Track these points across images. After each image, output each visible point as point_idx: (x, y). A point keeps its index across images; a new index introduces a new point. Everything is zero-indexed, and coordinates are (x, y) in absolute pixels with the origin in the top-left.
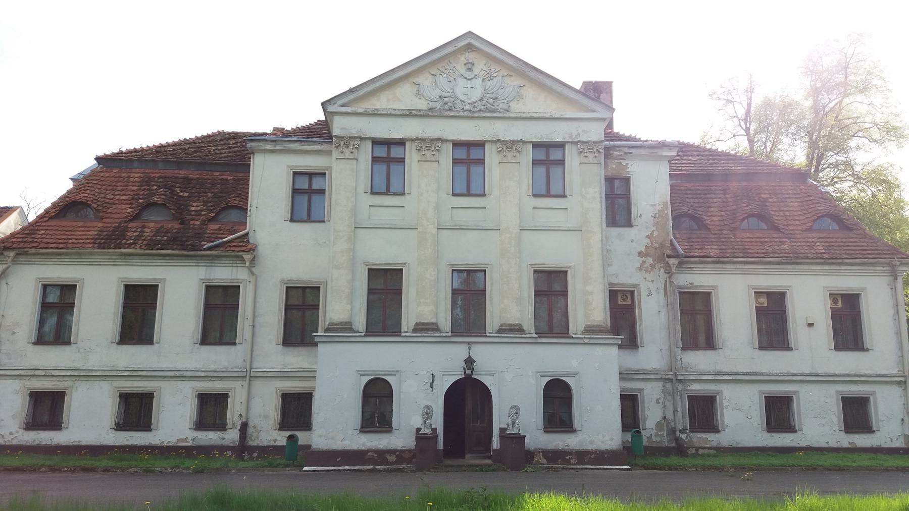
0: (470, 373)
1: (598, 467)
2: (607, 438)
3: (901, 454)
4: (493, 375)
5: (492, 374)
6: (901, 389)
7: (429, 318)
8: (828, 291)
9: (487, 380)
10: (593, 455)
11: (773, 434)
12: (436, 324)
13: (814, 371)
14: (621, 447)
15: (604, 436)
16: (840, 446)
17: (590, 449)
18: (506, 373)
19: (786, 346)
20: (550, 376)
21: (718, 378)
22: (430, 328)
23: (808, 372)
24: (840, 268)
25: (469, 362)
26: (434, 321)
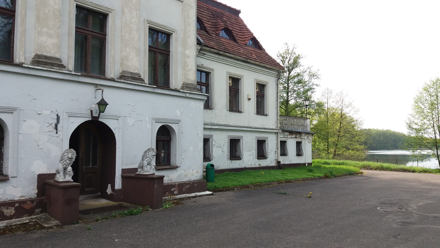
0: (97, 116)
1: (193, 195)
2: (195, 171)
3: (275, 169)
4: (118, 120)
5: (116, 118)
6: (276, 136)
7: (51, 52)
8: (256, 81)
9: (111, 124)
10: (188, 186)
11: (233, 161)
12: (59, 60)
13: (249, 125)
14: (202, 177)
15: (193, 170)
16: (255, 167)
17: (184, 181)
18: (128, 117)
19: (237, 110)
20: (161, 123)
21: (213, 127)
22: (56, 64)
23: (247, 126)
24: (262, 69)
25: (103, 104)
26: (57, 56)
